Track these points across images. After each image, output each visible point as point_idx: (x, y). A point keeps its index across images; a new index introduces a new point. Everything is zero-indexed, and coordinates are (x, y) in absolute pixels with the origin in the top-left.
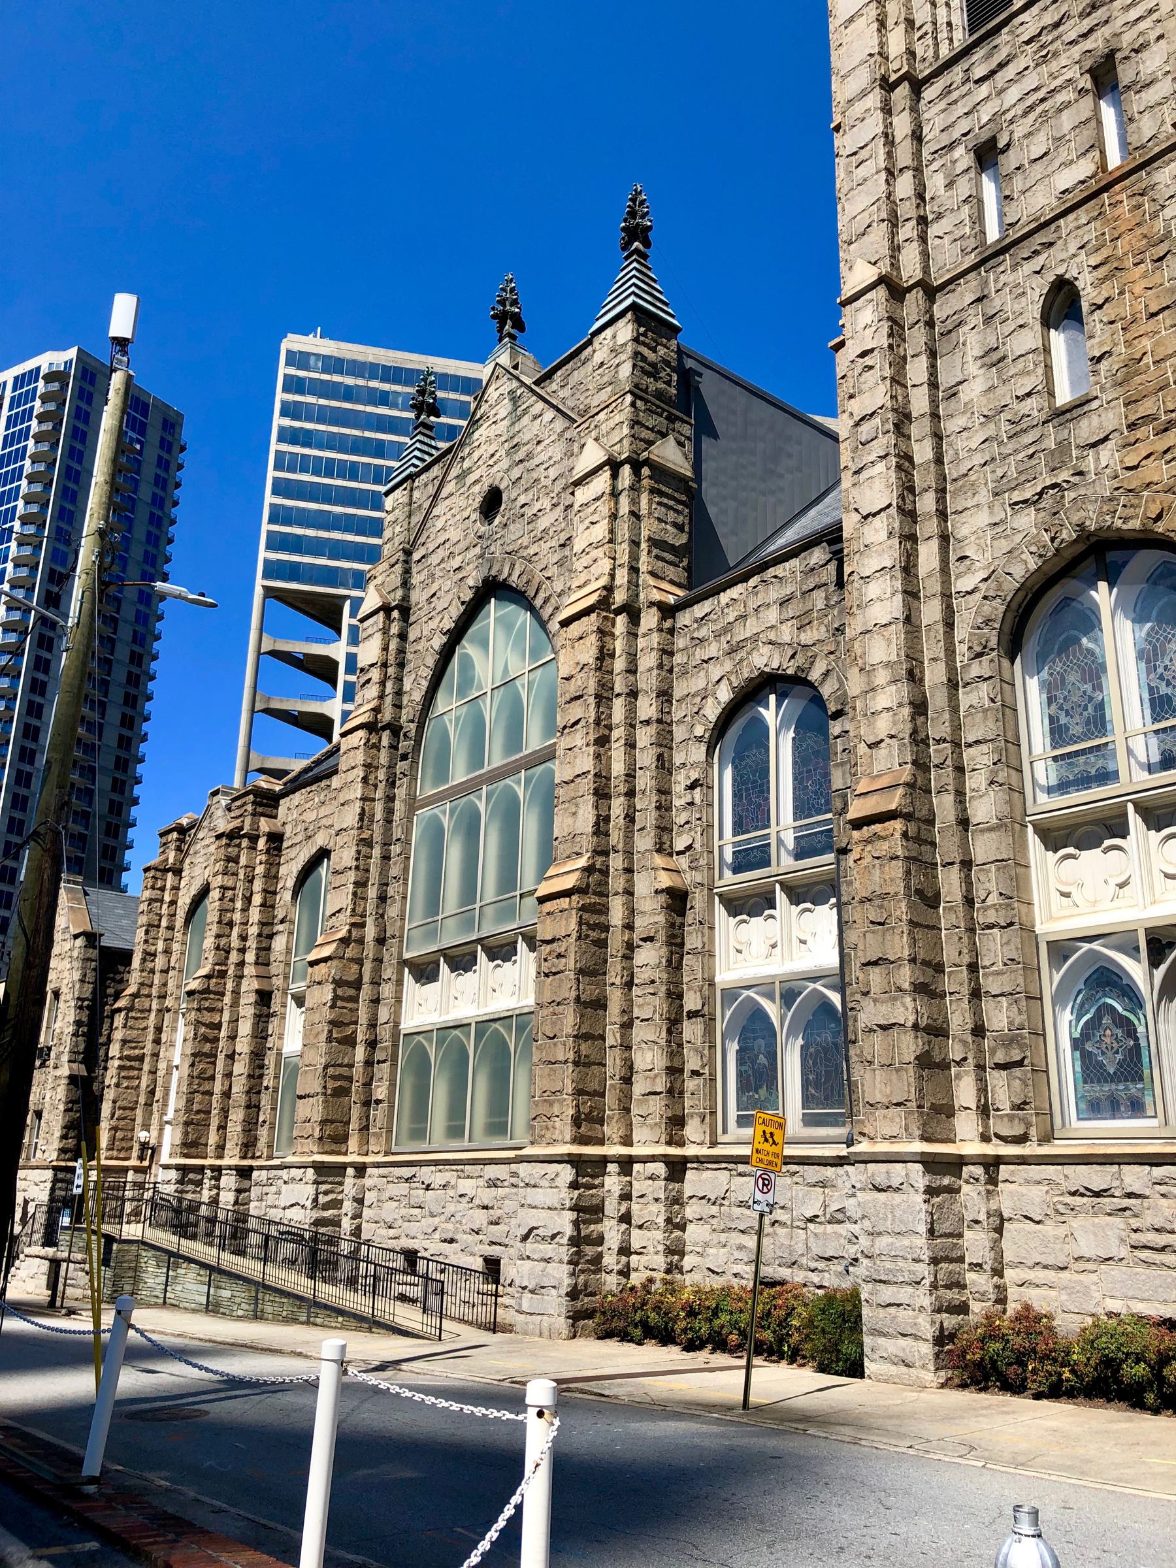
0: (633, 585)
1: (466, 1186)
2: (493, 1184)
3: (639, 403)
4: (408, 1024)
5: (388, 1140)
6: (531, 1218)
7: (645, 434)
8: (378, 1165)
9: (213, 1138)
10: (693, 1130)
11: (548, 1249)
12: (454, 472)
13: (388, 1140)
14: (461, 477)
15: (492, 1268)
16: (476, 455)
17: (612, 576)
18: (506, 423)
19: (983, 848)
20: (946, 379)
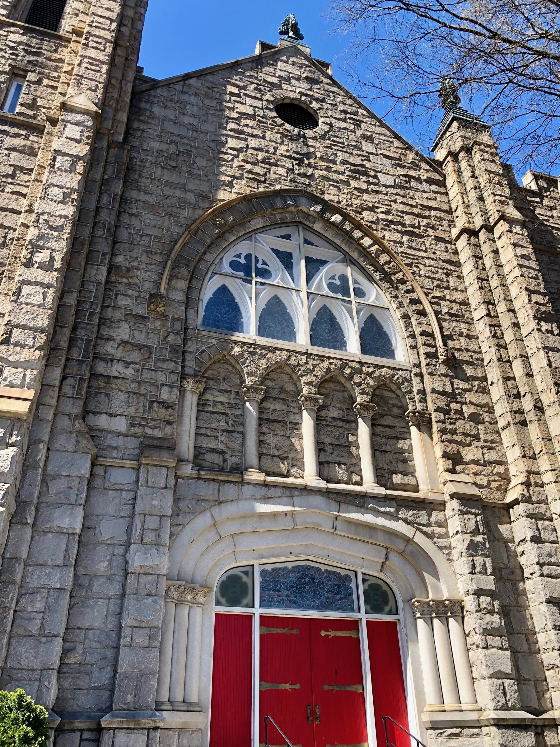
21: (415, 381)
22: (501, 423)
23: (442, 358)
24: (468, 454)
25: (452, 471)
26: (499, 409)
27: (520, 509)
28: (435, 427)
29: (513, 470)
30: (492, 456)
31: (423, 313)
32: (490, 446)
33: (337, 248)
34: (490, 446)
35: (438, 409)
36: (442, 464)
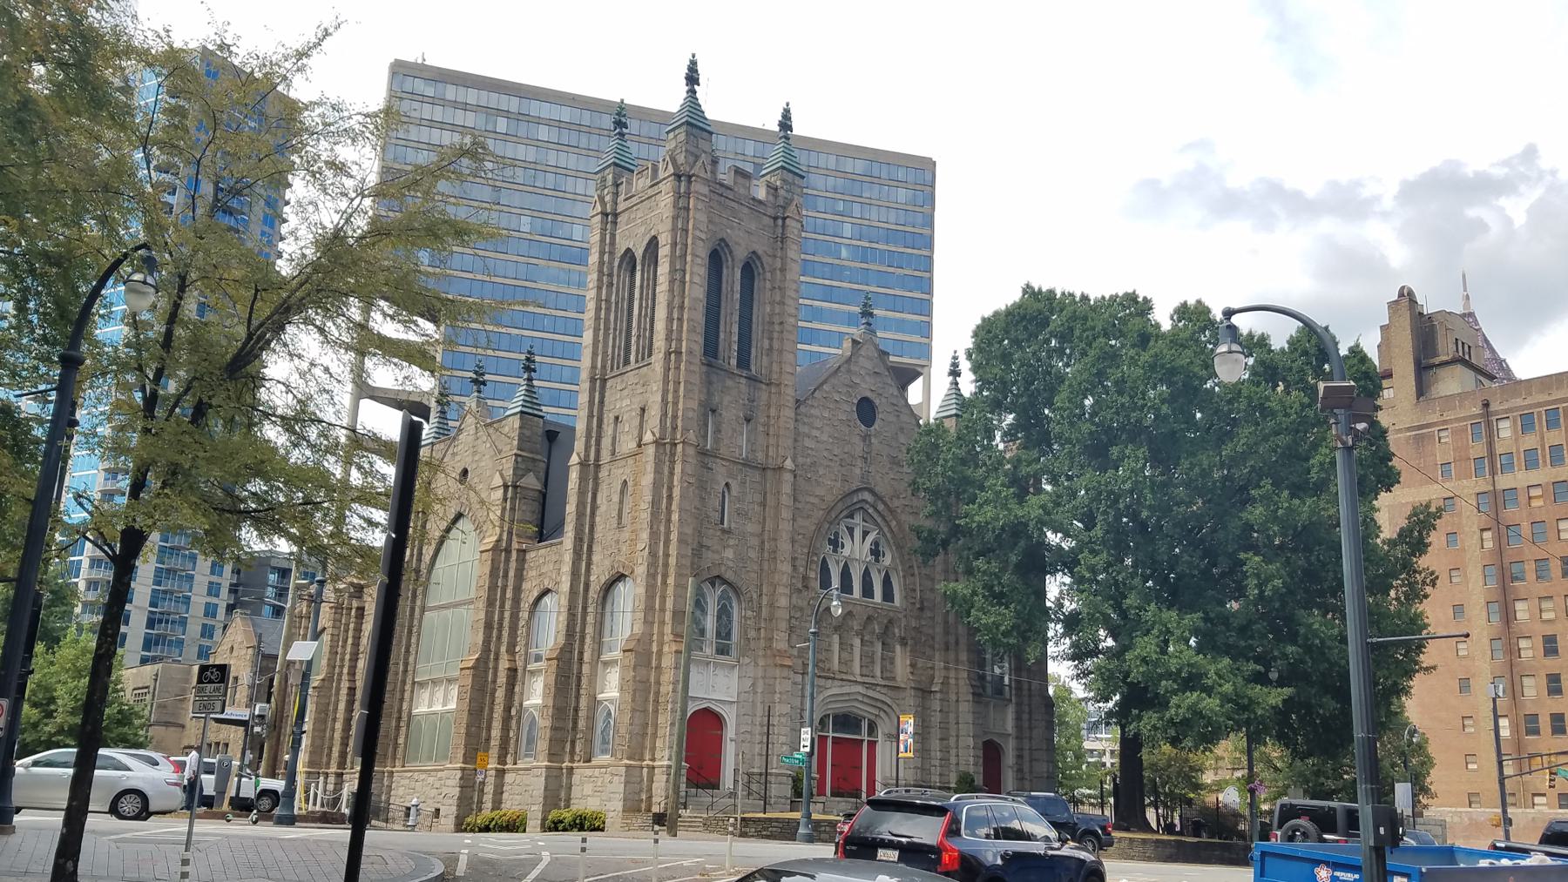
0: (510, 540)
1: (431, 780)
2: (440, 779)
3: (519, 459)
4: (415, 711)
5: (404, 761)
6: (445, 791)
7: (521, 473)
8: (398, 772)
9: (325, 759)
10: (509, 759)
11: (451, 801)
12: (450, 451)
13: (404, 761)
14: (454, 454)
15: (438, 810)
16: (460, 448)
17: (501, 535)
18: (472, 438)
19: (586, 669)
20: (599, 502)
21: (904, 620)
22: (937, 646)
23: (918, 606)
24: (919, 665)
25: (912, 673)
26: (937, 639)
27: (938, 696)
28: (908, 648)
29: (937, 673)
30: (930, 665)
31: (913, 575)
32: (930, 658)
33: (877, 524)
34: (930, 658)
35: (912, 638)
36: (909, 669)
